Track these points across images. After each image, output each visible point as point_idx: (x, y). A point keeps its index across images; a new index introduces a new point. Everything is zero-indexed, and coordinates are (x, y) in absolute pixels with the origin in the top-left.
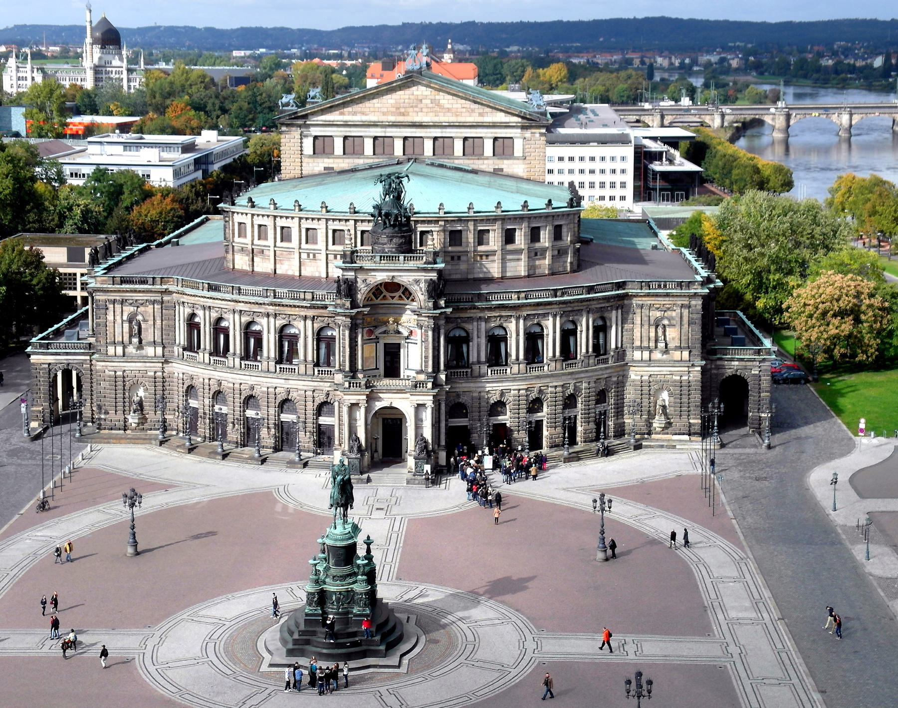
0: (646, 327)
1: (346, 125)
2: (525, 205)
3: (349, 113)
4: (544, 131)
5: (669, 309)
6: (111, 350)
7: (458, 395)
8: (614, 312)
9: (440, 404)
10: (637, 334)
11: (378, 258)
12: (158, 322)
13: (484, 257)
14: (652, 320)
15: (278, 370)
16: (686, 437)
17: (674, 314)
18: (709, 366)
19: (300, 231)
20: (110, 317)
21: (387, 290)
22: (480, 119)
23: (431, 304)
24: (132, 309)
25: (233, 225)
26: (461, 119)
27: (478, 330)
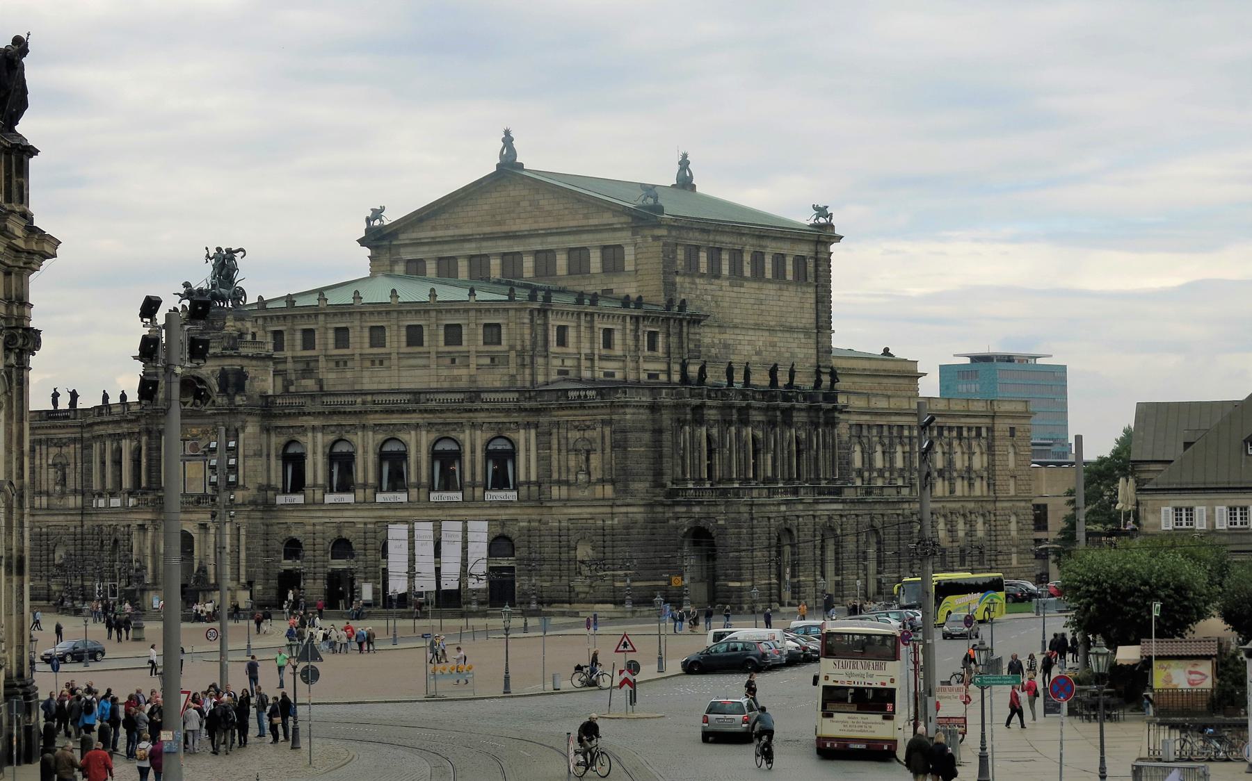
0: (564, 452)
1: (434, 242)
2: (433, 294)
4: (658, 232)
5: (588, 427)
7: (288, 528)
8: (522, 431)
9: (238, 529)
10: (555, 464)
12: (79, 465)
13: (377, 362)
16: (611, 606)
18: (667, 515)
20: (37, 462)
22: (584, 222)
26: (562, 224)
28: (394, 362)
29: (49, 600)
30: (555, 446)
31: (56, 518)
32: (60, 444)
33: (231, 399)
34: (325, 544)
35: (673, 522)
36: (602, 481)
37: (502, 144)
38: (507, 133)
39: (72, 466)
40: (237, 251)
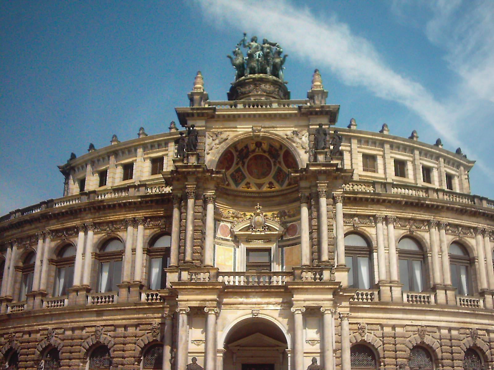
21: (251, 173)
34: (404, 352)
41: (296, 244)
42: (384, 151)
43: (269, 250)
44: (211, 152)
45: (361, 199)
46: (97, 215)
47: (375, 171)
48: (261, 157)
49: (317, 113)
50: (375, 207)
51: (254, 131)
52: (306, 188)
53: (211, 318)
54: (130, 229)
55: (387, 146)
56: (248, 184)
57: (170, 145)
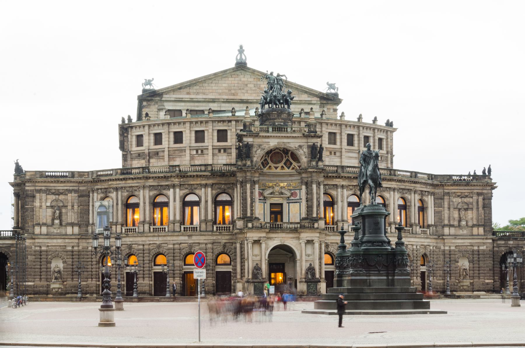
3: (194, 93)
6: (37, 230)
11: (270, 129)
12: (76, 207)
13: (333, 153)
14: (456, 204)
15: (182, 229)
16: (484, 293)
17: (471, 200)
19: (190, 133)
20: (37, 204)
21: (272, 161)
23: (314, 163)
24: (54, 197)
25: (131, 138)
27: (342, 196)
28: (344, 153)
29: (47, 294)
30: (446, 206)
31: (55, 241)
32: (58, 193)
33: (317, 163)
35: (497, 249)
36: (478, 226)
37: (238, 52)
38: (241, 47)
39: (70, 207)
40: (282, 76)
41: (297, 202)
42: (341, 130)
43: (281, 205)
44: (257, 155)
45: (330, 176)
46: (182, 180)
47: (335, 143)
48: (278, 153)
49: (312, 137)
50: (337, 180)
51: (278, 145)
52: (305, 178)
53: (263, 245)
54: (203, 189)
55: (344, 127)
56: (270, 167)
57: (209, 124)
